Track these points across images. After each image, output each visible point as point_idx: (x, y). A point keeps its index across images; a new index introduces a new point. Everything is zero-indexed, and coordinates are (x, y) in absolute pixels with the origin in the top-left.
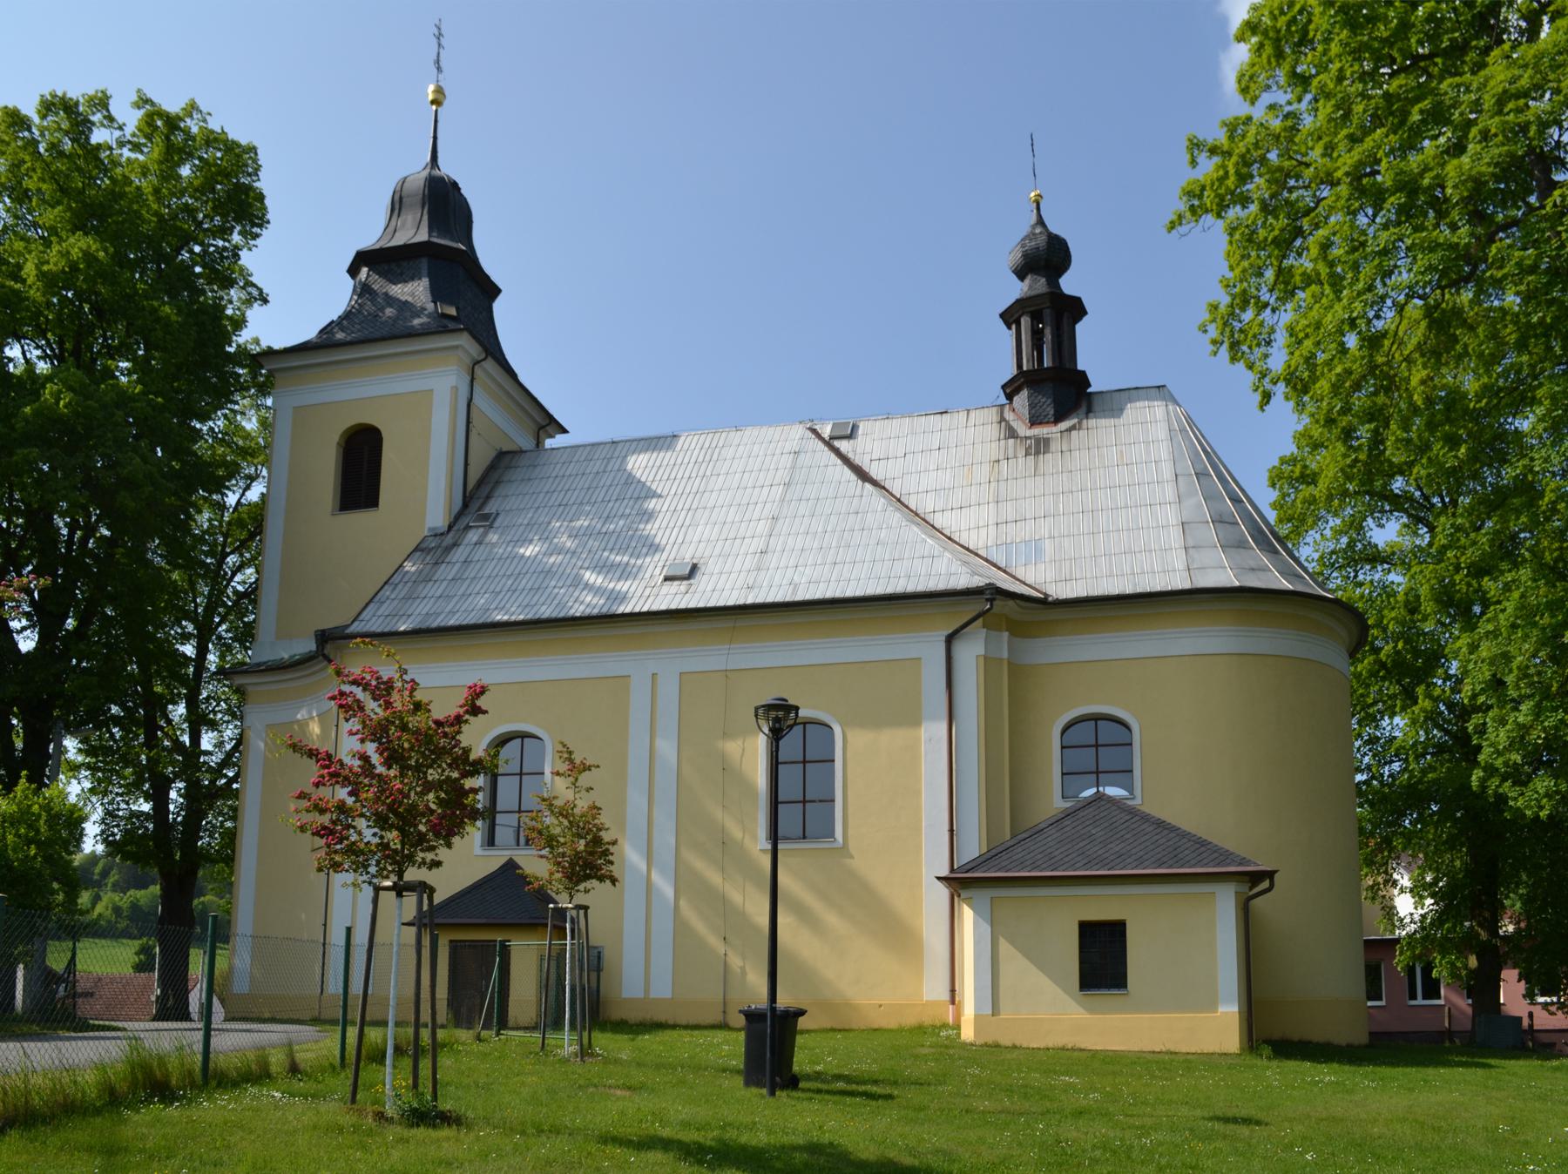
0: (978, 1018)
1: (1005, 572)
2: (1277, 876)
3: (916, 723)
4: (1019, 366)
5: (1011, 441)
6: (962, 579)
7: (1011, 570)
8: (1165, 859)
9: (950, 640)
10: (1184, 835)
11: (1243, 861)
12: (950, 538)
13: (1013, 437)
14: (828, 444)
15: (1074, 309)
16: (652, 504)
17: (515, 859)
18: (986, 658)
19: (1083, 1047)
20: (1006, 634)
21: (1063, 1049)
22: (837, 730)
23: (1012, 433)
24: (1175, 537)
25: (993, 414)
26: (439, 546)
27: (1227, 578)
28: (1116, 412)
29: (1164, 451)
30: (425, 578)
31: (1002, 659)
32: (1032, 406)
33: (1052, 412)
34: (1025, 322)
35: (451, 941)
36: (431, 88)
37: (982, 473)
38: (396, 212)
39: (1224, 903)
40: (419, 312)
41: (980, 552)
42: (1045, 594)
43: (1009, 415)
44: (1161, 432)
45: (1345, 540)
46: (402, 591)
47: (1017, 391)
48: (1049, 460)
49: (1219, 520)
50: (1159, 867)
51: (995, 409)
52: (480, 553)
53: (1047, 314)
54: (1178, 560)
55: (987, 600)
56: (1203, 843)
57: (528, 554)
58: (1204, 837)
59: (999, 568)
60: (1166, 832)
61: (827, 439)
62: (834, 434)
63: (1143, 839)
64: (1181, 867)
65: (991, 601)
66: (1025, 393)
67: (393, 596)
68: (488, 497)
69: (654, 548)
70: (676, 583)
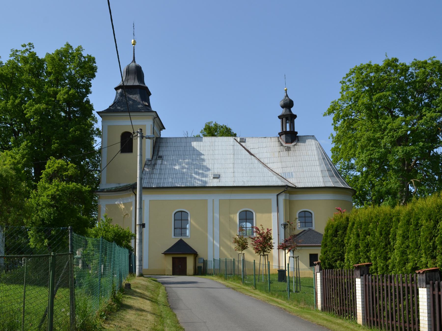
3: (271, 212)
5: (282, 147)
6: (280, 183)
7: (287, 179)
9: (277, 195)
15: (294, 116)
16: (202, 157)
17: (182, 239)
23: (282, 145)
24: (320, 174)
26: (151, 164)
27: (331, 184)
28: (304, 142)
29: (315, 152)
30: (152, 173)
32: (286, 139)
34: (284, 119)
35: (172, 257)
36: (133, 41)
37: (277, 154)
38: (128, 74)
40: (139, 103)
43: (280, 140)
47: (282, 135)
52: (163, 167)
53: (289, 118)
54: (321, 180)
57: (177, 168)
65: (287, 188)
66: (284, 136)
67: (146, 177)
68: (158, 151)
70: (216, 179)
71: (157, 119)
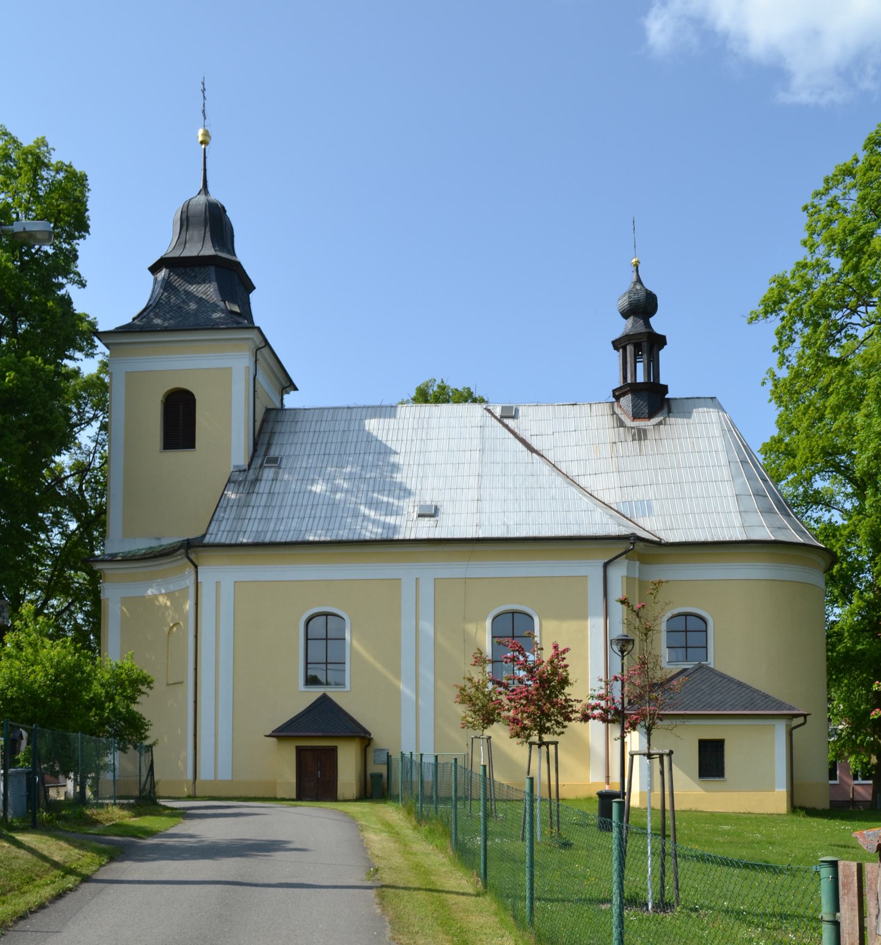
0: (641, 794)
1: (630, 520)
2: (808, 717)
3: (585, 617)
4: (625, 378)
5: (622, 429)
6: (614, 529)
7: (635, 520)
8: (747, 705)
9: (606, 566)
10: (755, 691)
11: (791, 708)
12: (591, 495)
13: (623, 427)
14: (500, 421)
15: (659, 341)
16: (393, 459)
17: (328, 694)
18: (627, 577)
19: (701, 809)
20: (638, 563)
21: (690, 811)
22: (536, 620)
23: (621, 424)
24: (732, 505)
25: (606, 408)
26: (245, 480)
27: (767, 534)
28: (687, 414)
29: (719, 444)
30: (244, 505)
31: (634, 578)
32: (634, 406)
33: (647, 411)
34: (630, 349)
35: (297, 747)
36: (201, 131)
37: (606, 450)
38: (185, 227)
39: (780, 730)
40: (215, 307)
41: (612, 506)
42: (659, 538)
43: (618, 410)
44: (716, 431)
45: (801, 489)
46: (231, 514)
47: (624, 394)
48: (648, 445)
49: (758, 494)
50: (745, 709)
51: (608, 404)
52: (278, 487)
53: (645, 345)
54: (736, 520)
55: (631, 543)
56: (766, 696)
57: (318, 490)
58: (767, 693)
59: (627, 518)
60: (744, 689)
61: (499, 417)
62: (504, 415)
63: (732, 693)
64: (757, 710)
65: (633, 544)
66: (629, 397)
67: (226, 516)
68: (269, 445)
69: (407, 493)
70: (427, 519)
71: (265, 351)
